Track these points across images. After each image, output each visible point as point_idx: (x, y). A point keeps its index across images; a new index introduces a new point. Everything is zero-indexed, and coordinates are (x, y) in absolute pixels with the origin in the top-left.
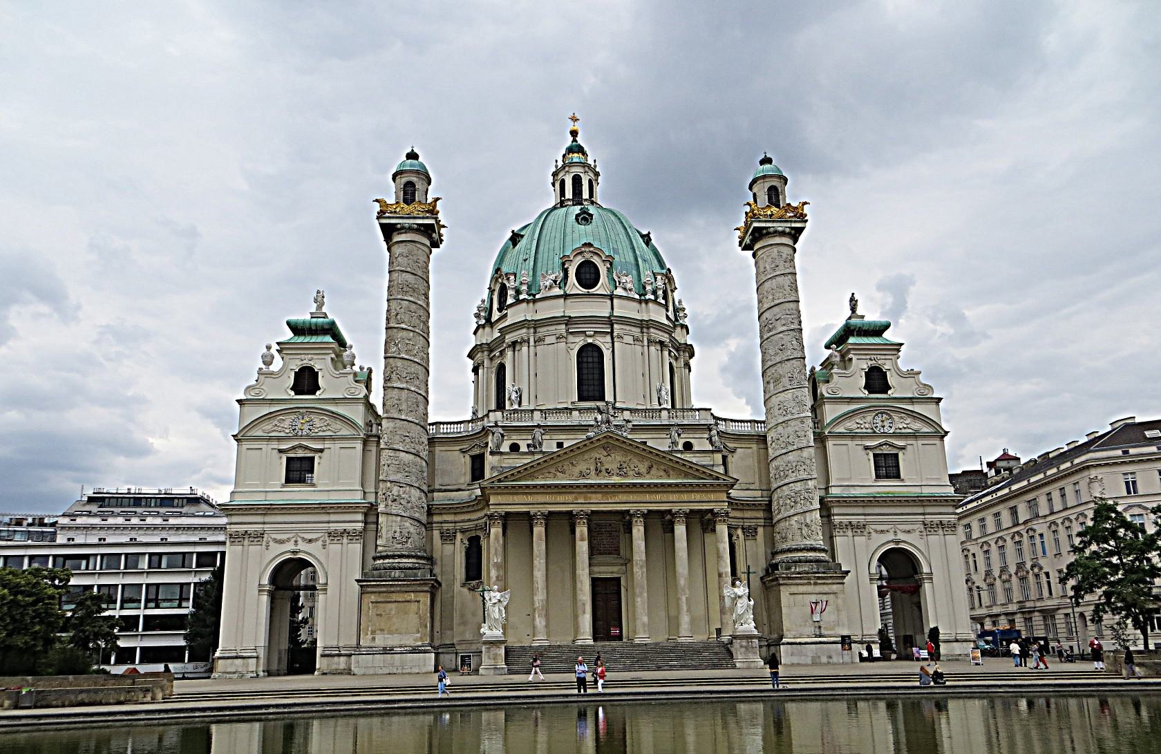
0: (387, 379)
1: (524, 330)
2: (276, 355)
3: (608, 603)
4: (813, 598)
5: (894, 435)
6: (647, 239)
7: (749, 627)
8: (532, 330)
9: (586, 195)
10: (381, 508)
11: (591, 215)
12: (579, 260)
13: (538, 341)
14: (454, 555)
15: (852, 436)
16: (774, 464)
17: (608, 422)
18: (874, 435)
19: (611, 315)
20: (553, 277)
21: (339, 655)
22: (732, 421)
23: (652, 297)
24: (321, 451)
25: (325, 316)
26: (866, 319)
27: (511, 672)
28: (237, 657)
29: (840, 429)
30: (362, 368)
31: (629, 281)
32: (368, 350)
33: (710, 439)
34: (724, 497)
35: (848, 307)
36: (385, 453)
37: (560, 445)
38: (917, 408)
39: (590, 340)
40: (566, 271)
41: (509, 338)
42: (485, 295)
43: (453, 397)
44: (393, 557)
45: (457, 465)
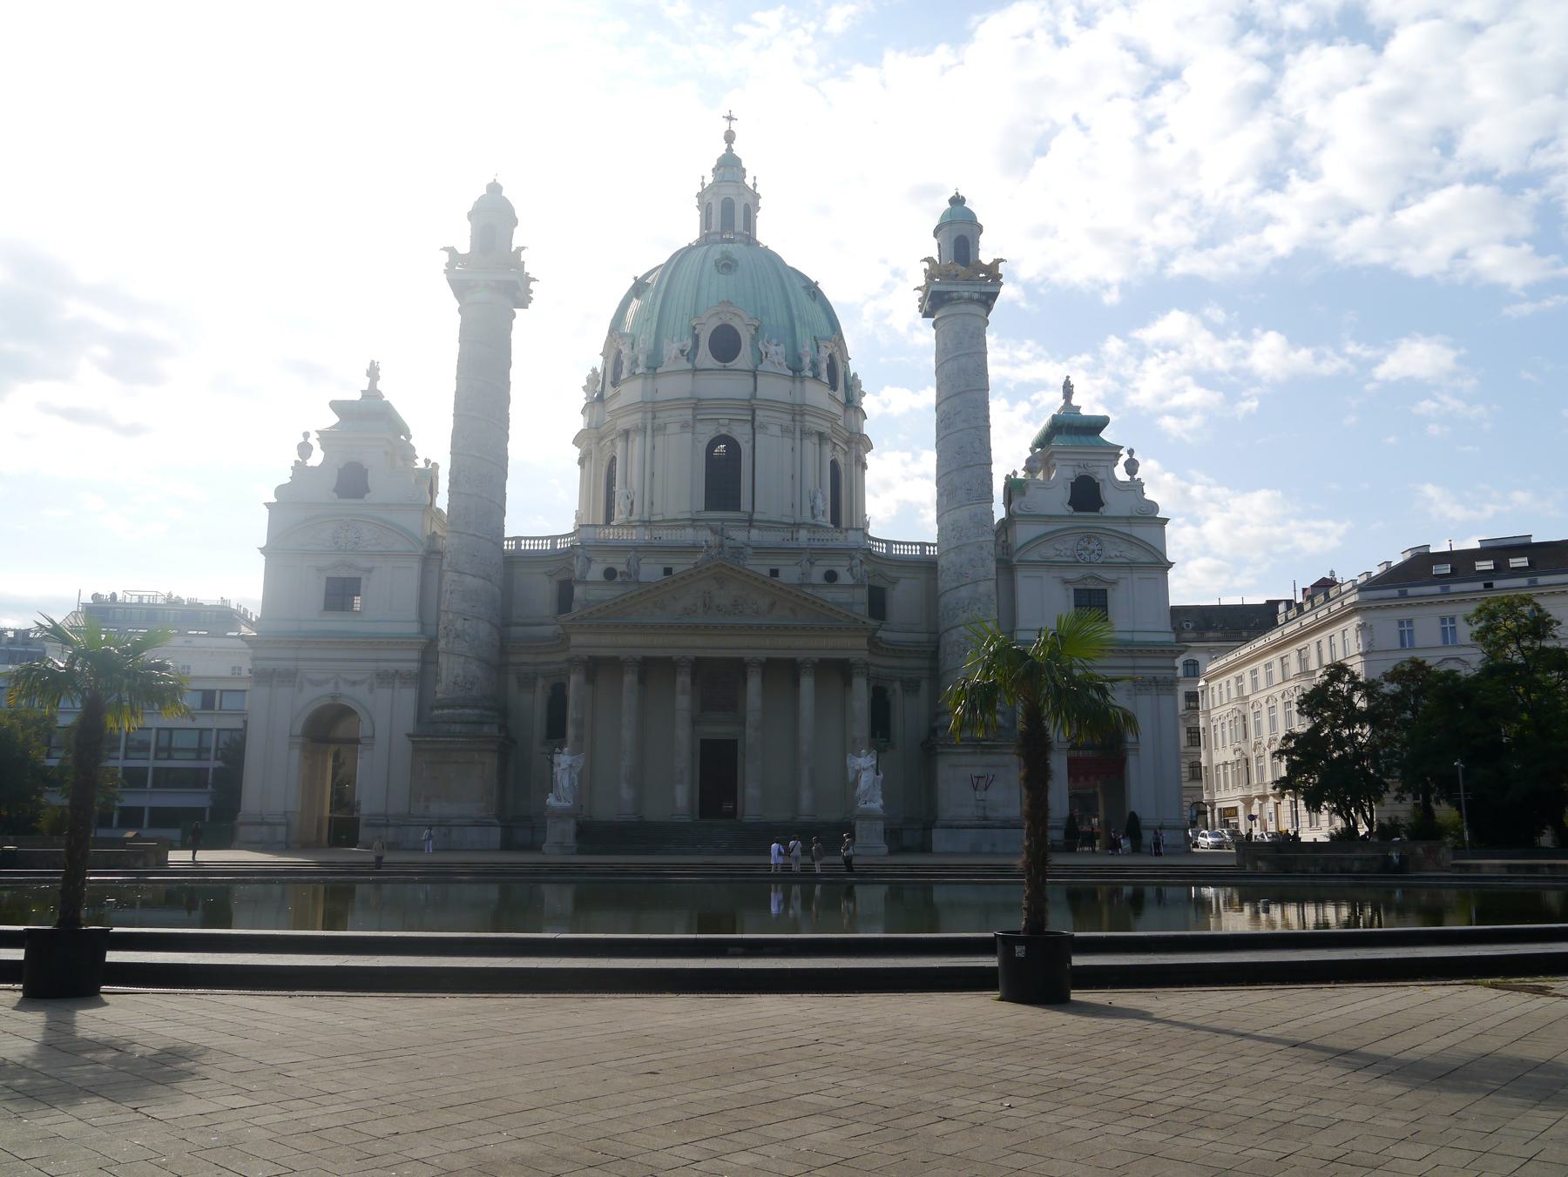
0: (453, 482)
1: (640, 415)
2: (316, 445)
3: (718, 768)
4: (978, 772)
5: (1108, 565)
6: (813, 290)
7: (877, 804)
8: (650, 415)
9: (739, 225)
10: (442, 644)
11: (735, 262)
12: (714, 323)
13: (659, 429)
14: (532, 706)
15: (1049, 564)
16: (943, 600)
17: (722, 546)
18: (1075, 564)
19: (754, 396)
20: (676, 346)
21: (387, 826)
22: (896, 543)
23: (810, 374)
24: (370, 570)
25: (379, 395)
26: (1084, 412)
27: (580, 852)
28: (261, 824)
29: (1034, 556)
30: (427, 461)
31: (777, 353)
32: (432, 441)
33: (851, 569)
34: (863, 642)
35: (1061, 394)
36: (450, 576)
37: (668, 571)
38: (1139, 532)
39: (724, 431)
40: (696, 338)
41: (623, 423)
42: (598, 363)
43: (545, 499)
44: (453, 707)
45: (540, 593)
